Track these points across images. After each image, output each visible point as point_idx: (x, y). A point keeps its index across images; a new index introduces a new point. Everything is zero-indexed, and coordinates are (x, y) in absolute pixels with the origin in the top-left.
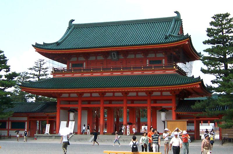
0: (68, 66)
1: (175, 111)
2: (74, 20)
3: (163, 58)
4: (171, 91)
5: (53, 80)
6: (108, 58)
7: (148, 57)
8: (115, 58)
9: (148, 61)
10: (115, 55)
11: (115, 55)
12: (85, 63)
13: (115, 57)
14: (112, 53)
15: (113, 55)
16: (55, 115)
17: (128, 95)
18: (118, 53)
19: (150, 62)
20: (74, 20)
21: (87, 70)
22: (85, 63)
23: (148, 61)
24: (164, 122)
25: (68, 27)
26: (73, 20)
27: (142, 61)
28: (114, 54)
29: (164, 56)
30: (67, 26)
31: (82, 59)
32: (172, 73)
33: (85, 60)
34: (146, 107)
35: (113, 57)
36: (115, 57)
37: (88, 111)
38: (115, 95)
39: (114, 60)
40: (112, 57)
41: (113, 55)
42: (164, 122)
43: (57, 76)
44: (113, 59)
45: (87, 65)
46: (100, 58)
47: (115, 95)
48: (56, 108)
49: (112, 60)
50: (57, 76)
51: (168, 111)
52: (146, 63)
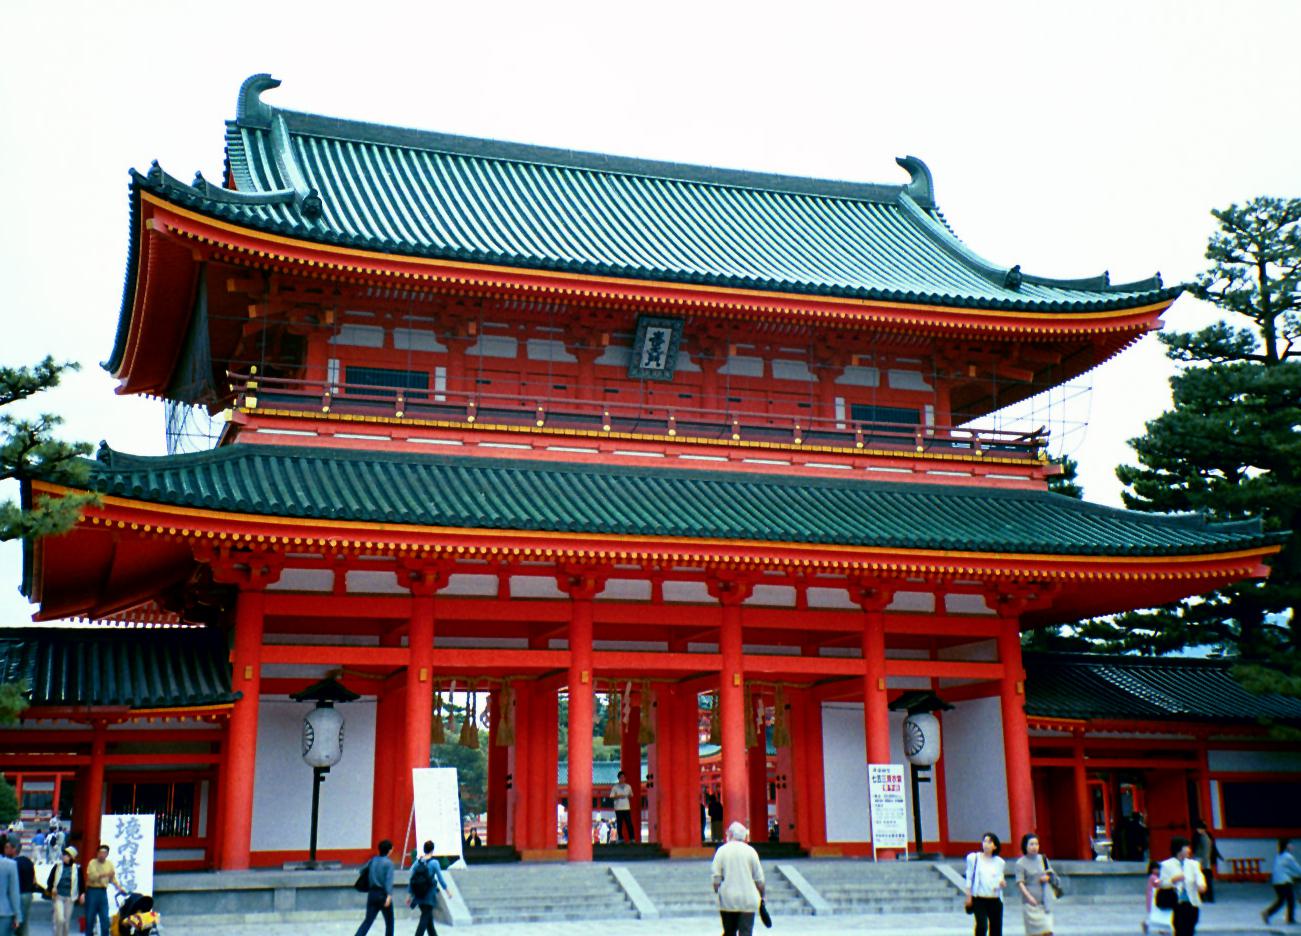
4: (989, 588)
6: (601, 361)
7: (841, 380)
8: (653, 365)
10: (664, 347)
11: (664, 347)
14: (651, 332)
15: (648, 345)
19: (855, 412)
28: (658, 336)
34: (711, 680)
35: (645, 359)
36: (657, 359)
37: (379, 701)
39: (643, 375)
40: (640, 355)
41: (648, 345)
44: (637, 367)
46: (548, 351)
48: (225, 673)
52: (834, 414)
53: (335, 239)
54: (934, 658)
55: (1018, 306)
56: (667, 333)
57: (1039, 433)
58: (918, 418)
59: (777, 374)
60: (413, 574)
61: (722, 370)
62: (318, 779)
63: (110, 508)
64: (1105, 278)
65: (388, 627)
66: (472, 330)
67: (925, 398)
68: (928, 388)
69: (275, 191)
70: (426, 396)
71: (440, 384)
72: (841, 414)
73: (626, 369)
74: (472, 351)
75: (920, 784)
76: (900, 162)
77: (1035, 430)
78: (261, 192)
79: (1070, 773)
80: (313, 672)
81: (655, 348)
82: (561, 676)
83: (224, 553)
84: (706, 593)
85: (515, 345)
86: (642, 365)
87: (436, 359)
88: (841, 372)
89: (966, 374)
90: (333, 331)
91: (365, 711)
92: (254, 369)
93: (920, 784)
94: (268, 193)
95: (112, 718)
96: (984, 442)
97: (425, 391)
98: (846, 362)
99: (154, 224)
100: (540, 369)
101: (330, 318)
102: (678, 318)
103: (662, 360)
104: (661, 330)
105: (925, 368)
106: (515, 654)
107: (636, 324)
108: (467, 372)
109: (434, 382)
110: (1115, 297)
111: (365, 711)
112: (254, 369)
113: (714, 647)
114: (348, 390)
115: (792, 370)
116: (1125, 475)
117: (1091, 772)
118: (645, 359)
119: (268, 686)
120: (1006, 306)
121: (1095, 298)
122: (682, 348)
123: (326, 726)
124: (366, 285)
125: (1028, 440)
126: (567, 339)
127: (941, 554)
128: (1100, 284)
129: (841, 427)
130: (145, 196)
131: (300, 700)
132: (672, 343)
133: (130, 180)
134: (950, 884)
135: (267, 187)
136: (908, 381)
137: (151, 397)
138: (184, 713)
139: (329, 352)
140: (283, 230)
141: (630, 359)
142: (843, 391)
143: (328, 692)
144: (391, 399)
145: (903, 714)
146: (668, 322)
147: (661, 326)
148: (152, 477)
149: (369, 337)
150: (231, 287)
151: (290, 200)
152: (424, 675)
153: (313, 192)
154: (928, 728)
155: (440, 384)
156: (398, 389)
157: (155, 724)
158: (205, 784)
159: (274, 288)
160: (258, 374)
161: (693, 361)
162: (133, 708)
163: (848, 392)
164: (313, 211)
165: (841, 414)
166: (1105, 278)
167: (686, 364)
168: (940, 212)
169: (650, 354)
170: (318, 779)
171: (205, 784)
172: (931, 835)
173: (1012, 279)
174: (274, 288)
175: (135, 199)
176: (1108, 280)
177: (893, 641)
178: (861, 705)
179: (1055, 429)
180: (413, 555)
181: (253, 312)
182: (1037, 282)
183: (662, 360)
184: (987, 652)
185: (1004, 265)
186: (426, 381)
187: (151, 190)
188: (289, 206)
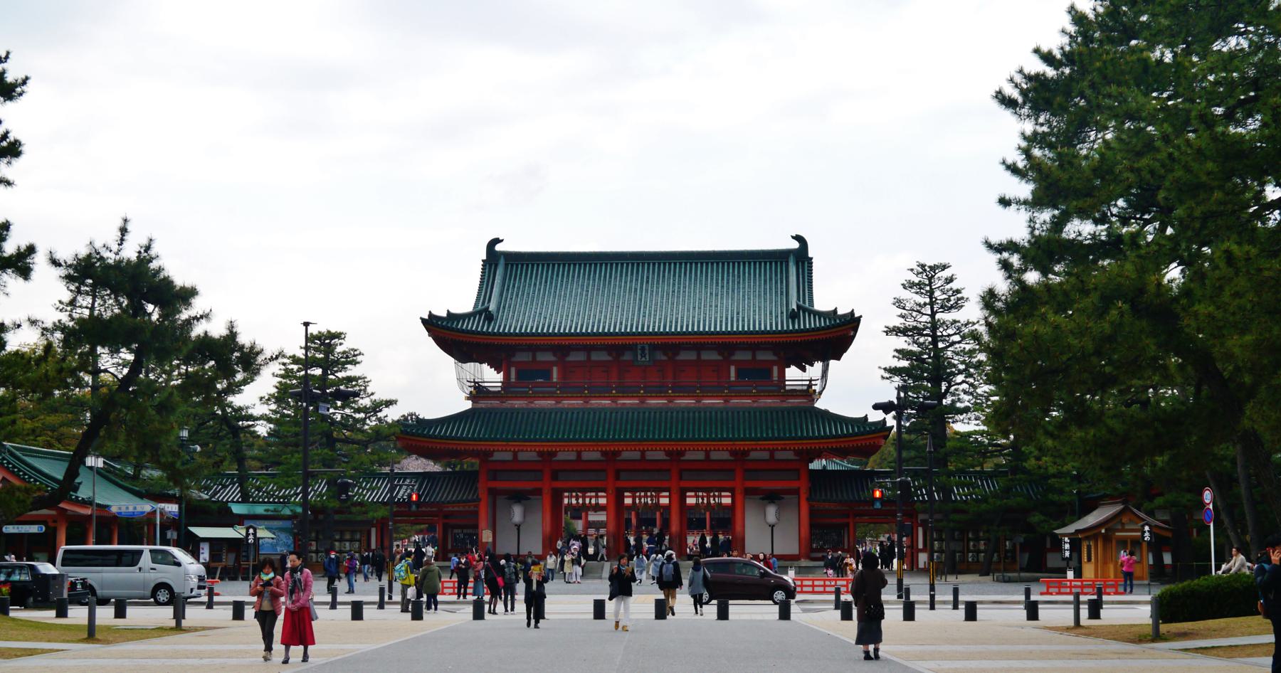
0: (507, 377)
1: (808, 499)
2: (502, 241)
3: (774, 363)
5: (474, 414)
9: (733, 369)
10: (647, 352)
11: (647, 352)
12: (555, 369)
13: (643, 355)
14: (639, 347)
15: (639, 352)
16: (472, 508)
17: (682, 458)
18: (654, 348)
20: (502, 241)
21: (567, 389)
22: (555, 369)
23: (733, 369)
24: (772, 526)
25: (485, 258)
26: (497, 241)
27: (721, 368)
29: (774, 358)
30: (483, 255)
31: (549, 357)
32: (802, 405)
35: (639, 357)
41: (639, 352)
42: (772, 526)
43: (483, 404)
45: (564, 374)
47: (648, 458)
50: (483, 404)
56: (647, 347)
62: (519, 529)
64: (835, 311)
76: (793, 237)
95: (448, 507)
108: (566, 369)
115: (713, 356)
118: (639, 357)
127: (731, 443)
132: (649, 350)
136: (763, 356)
142: (734, 363)
157: (461, 509)
166: (835, 311)
170: (519, 529)
183: (647, 357)
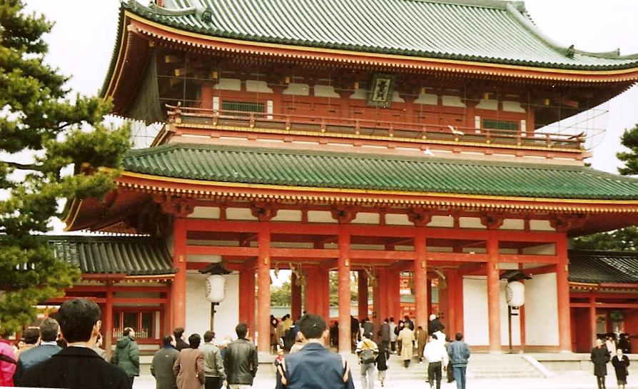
3: (521, 116)
6: (353, 97)
7: (478, 107)
11: (386, 89)
14: (379, 81)
19: (485, 124)
28: (383, 84)
33: (272, 92)
35: (376, 95)
36: (382, 96)
38: (388, 222)
39: (376, 104)
41: (377, 89)
46: (326, 92)
47: (388, 222)
49: (370, 103)
51: (528, 278)
53: (221, 34)
54: (520, 253)
55: (573, 68)
56: (388, 82)
57: (580, 135)
58: (518, 127)
59: (444, 104)
60: (259, 210)
61: (417, 102)
63: (125, 177)
65: (244, 238)
66: (287, 81)
67: (521, 116)
68: (523, 111)
69: (186, 9)
70: (263, 116)
71: (270, 110)
72: (478, 125)
73: (367, 101)
74: (286, 92)
75: (512, 316)
77: (578, 134)
78: (179, 9)
79: (588, 310)
80: (215, 259)
81: (381, 90)
82: (334, 263)
83: (169, 198)
84: (407, 220)
85: (437, 99)
86: (374, 99)
87: (266, 97)
88: (478, 103)
89: (543, 104)
90: (216, 82)
91: (234, 278)
92: (179, 103)
93: (512, 316)
94: (182, 10)
96: (553, 140)
97: (262, 114)
98: (481, 97)
99: (130, 28)
100: (322, 102)
101: (215, 75)
102: (394, 73)
103: (385, 97)
104: (384, 80)
105: (522, 100)
106: (306, 250)
107: (372, 76)
108: (284, 103)
109: (267, 109)
110: (623, 63)
111: (234, 278)
112: (179, 103)
113: (411, 248)
114: (223, 114)
115: (452, 102)
116: (622, 157)
117: (599, 310)
118: (376, 95)
119: (190, 266)
120: (568, 67)
121: (613, 63)
122: (396, 89)
123: (217, 284)
124: (231, 59)
125: (575, 139)
126: (335, 84)
128: (615, 55)
129: (478, 132)
130: (127, 13)
131: (203, 273)
133: (120, 6)
134: (531, 365)
135: (182, 7)
136: (512, 108)
137: (115, 116)
138: (137, 279)
139: (214, 93)
140: (194, 30)
141: (368, 95)
142: (479, 112)
143: (217, 269)
144: (248, 118)
145: (505, 281)
146: (388, 76)
147: (385, 78)
148: (135, 160)
149: (234, 85)
150: (167, 61)
151: (194, 13)
152: (267, 261)
153: (209, 8)
154: (517, 289)
155: (270, 110)
156: (251, 113)
158: (158, 314)
159: (187, 61)
160: (181, 106)
161: (401, 96)
162: (127, 275)
163: (482, 113)
164: (208, 20)
165: (478, 125)
167: (397, 99)
168: (528, 14)
169: (379, 93)
171: (158, 314)
172: (516, 341)
173: (570, 53)
174: (187, 61)
175: (122, 15)
176: (619, 53)
177: (503, 245)
178: (485, 277)
179: (589, 133)
180: (353, 204)
181: (177, 73)
182: (583, 54)
183: (385, 97)
184: (550, 251)
185: (566, 45)
186: (263, 108)
187: (130, 10)
188: (194, 15)
